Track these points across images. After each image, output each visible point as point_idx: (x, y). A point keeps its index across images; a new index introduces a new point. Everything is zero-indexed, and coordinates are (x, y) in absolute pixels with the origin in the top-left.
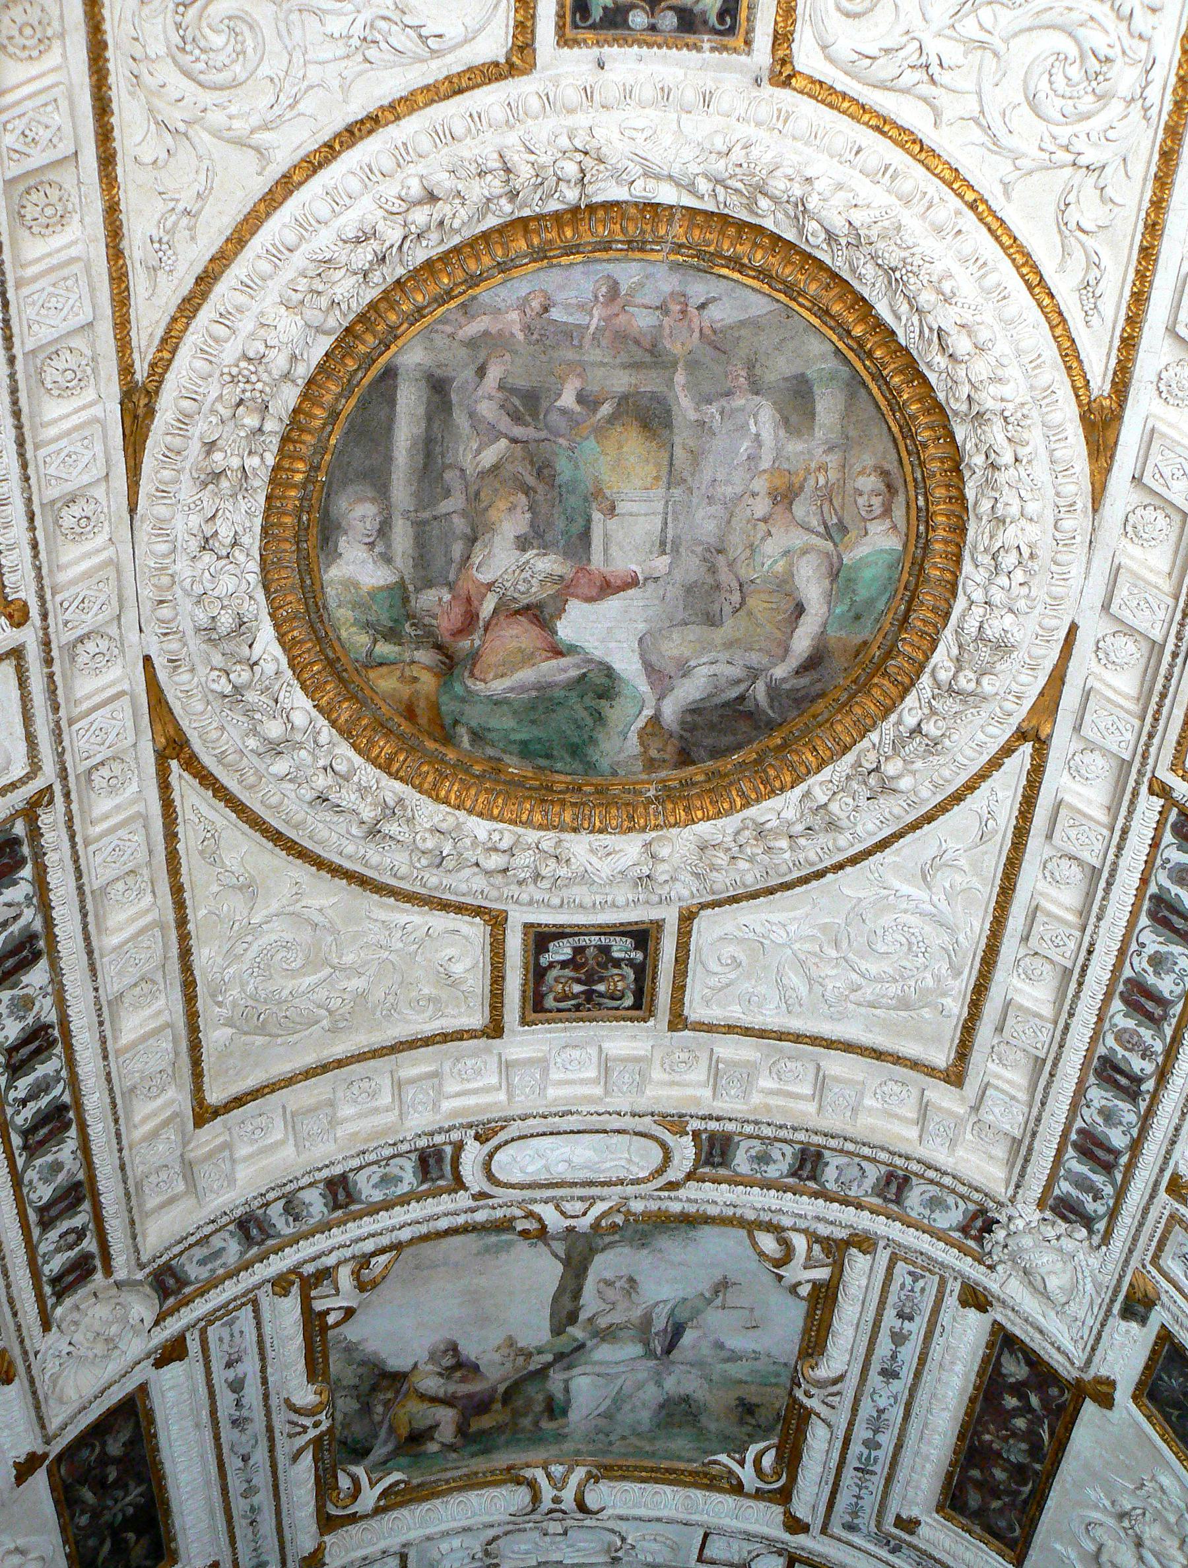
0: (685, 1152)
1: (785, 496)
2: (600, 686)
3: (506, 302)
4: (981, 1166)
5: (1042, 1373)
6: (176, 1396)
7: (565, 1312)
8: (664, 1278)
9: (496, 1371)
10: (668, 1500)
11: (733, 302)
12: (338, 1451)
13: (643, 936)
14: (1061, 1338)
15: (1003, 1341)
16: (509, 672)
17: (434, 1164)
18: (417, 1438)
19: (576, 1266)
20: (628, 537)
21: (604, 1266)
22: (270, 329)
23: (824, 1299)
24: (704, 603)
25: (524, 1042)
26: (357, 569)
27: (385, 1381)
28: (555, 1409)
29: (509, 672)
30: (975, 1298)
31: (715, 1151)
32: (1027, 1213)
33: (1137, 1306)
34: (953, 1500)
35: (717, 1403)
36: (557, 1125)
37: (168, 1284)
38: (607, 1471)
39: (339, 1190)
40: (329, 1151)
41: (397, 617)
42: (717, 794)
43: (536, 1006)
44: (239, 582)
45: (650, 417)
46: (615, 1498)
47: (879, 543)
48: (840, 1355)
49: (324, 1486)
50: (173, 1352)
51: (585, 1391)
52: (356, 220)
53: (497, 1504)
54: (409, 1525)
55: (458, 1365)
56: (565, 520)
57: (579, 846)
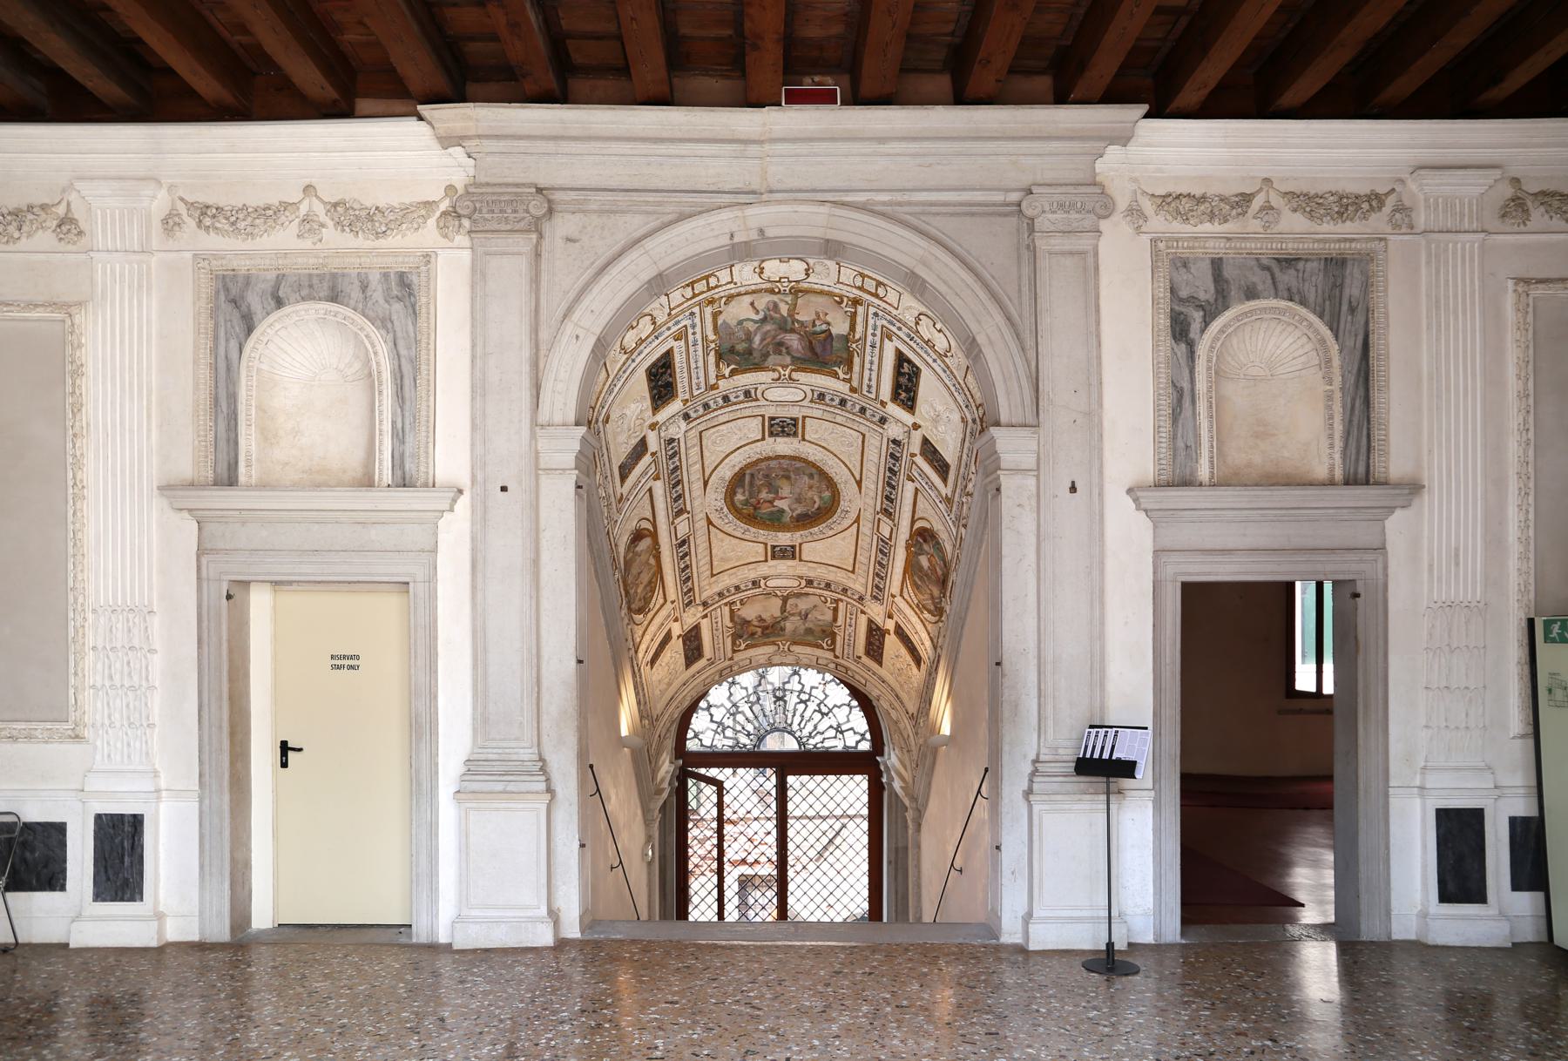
0: (804, 583)
1: (811, 487)
2: (782, 511)
3: (763, 465)
4: (861, 589)
5: (878, 628)
6: (705, 624)
7: (783, 609)
8: (803, 604)
9: (769, 621)
10: (808, 650)
11: (799, 465)
12: (736, 637)
13: (793, 547)
14: (879, 620)
15: (870, 621)
16: (765, 510)
17: (754, 583)
18: (753, 634)
19: (785, 600)
20: (786, 490)
21: (790, 602)
22: (726, 472)
23: (836, 610)
24: (799, 500)
25: (771, 563)
26: (739, 497)
27: (747, 623)
28: (783, 629)
29: (765, 510)
30: (863, 612)
31: (810, 582)
32: (868, 597)
33: (890, 617)
34: (867, 653)
35: (818, 629)
36: (778, 576)
37: (705, 604)
38: (795, 643)
39: (737, 588)
40: (735, 581)
41: (746, 503)
42: (804, 527)
43: (774, 557)
44: (721, 504)
45: (788, 478)
46: (794, 648)
47: (827, 494)
48: (840, 621)
49: (734, 643)
50: (705, 616)
51: (789, 626)
52: (738, 460)
53: (770, 649)
54: (752, 652)
55: (761, 619)
56: (774, 490)
57: (780, 534)
